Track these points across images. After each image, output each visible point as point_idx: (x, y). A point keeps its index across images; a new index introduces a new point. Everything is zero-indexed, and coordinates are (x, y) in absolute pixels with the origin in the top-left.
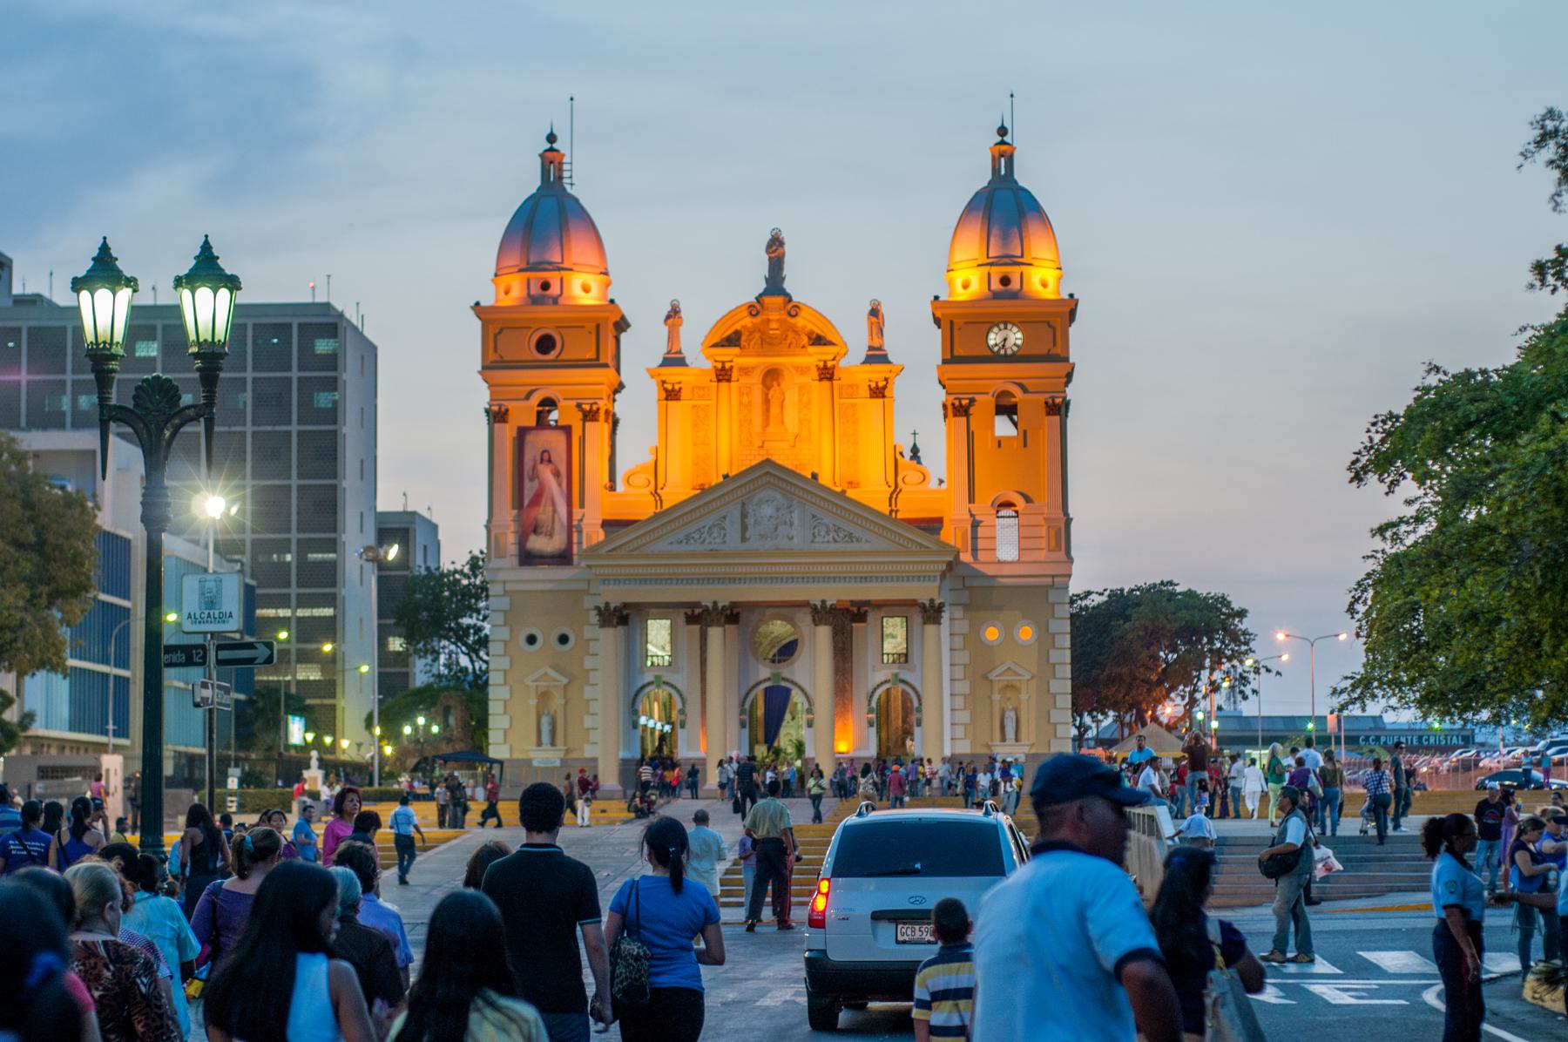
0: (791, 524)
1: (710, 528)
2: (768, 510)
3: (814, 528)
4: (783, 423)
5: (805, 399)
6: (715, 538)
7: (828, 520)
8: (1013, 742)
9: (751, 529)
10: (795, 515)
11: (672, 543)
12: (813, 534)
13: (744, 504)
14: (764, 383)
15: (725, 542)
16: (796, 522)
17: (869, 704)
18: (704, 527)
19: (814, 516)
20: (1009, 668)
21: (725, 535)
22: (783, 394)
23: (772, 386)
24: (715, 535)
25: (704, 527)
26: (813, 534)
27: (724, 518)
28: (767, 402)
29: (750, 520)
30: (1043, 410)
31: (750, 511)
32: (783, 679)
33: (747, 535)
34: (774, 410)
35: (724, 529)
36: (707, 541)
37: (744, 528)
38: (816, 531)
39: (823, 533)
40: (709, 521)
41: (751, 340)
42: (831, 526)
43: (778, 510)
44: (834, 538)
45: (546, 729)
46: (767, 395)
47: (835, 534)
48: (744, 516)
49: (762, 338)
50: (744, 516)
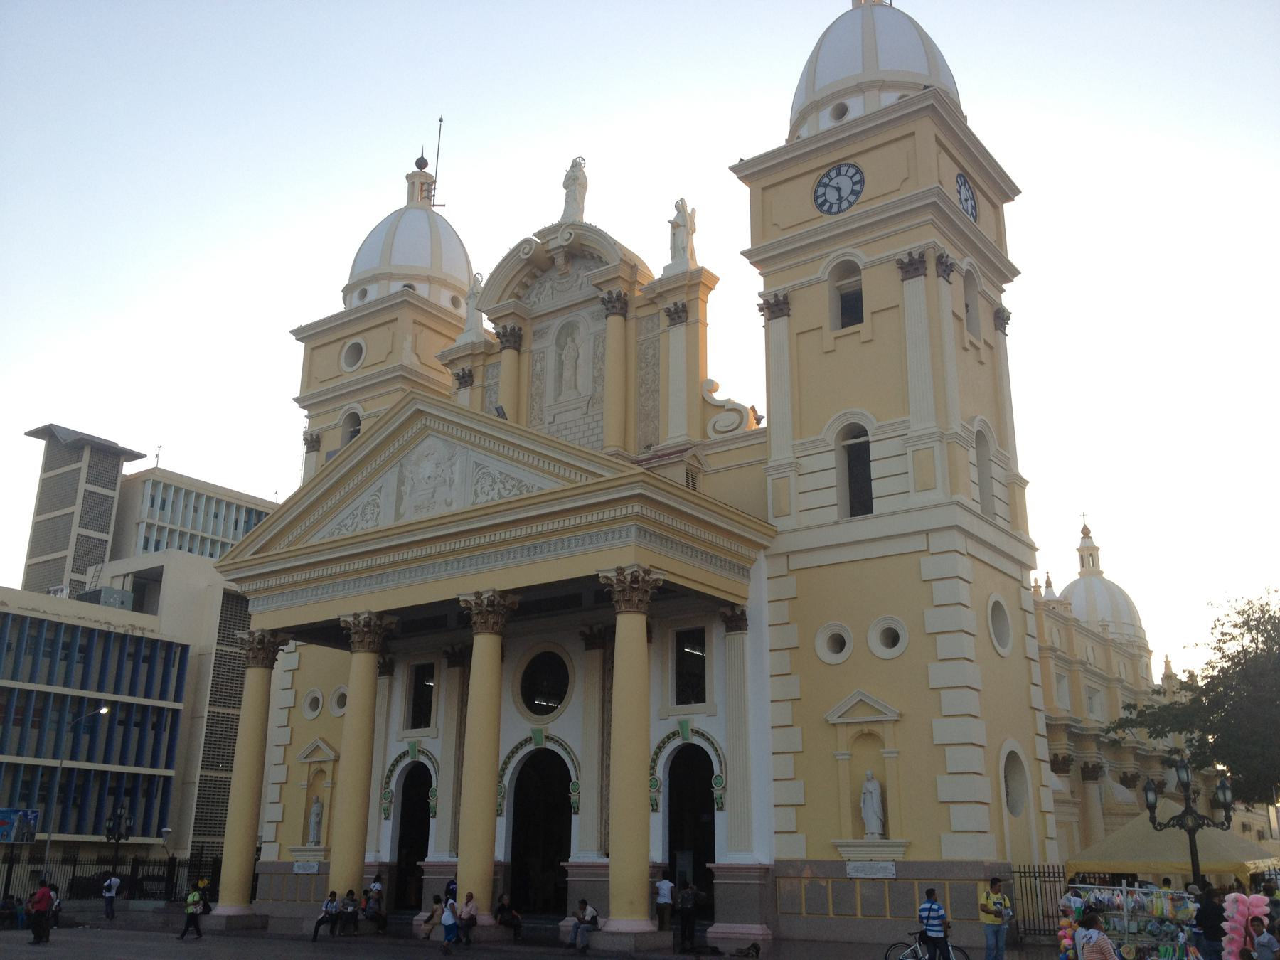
0: (452, 482)
1: (364, 508)
2: (427, 468)
3: (477, 483)
4: (576, 387)
5: (601, 350)
6: (367, 522)
7: (495, 466)
8: (877, 839)
9: (406, 498)
10: (457, 468)
11: (324, 537)
12: (476, 490)
13: (401, 466)
14: (558, 339)
15: (378, 525)
16: (457, 477)
17: (652, 775)
18: (357, 509)
19: (478, 465)
20: (861, 700)
21: (378, 514)
22: (577, 350)
23: (567, 344)
24: (368, 516)
25: (357, 509)
26: (476, 490)
27: (380, 490)
28: (561, 363)
29: (406, 488)
30: (897, 275)
31: (407, 474)
32: (547, 737)
33: (402, 510)
34: (567, 374)
35: (378, 507)
36: (360, 527)
37: (400, 498)
38: (479, 487)
39: (486, 488)
40: (364, 498)
41: (541, 294)
42: (497, 475)
43: (437, 465)
44: (499, 493)
45: (313, 819)
46: (561, 355)
47: (501, 486)
48: (401, 482)
49: (552, 287)
50: (401, 482)
